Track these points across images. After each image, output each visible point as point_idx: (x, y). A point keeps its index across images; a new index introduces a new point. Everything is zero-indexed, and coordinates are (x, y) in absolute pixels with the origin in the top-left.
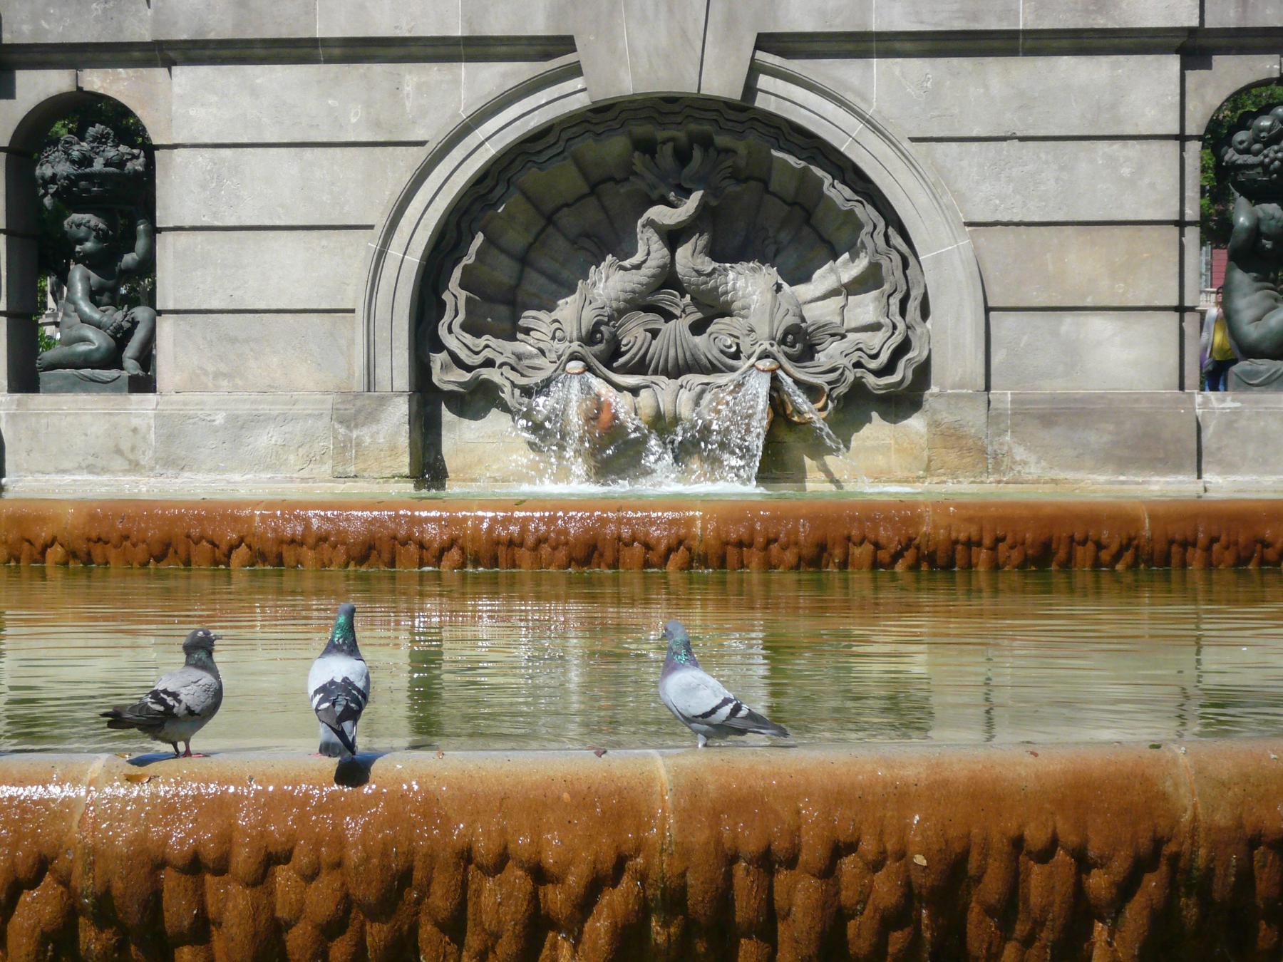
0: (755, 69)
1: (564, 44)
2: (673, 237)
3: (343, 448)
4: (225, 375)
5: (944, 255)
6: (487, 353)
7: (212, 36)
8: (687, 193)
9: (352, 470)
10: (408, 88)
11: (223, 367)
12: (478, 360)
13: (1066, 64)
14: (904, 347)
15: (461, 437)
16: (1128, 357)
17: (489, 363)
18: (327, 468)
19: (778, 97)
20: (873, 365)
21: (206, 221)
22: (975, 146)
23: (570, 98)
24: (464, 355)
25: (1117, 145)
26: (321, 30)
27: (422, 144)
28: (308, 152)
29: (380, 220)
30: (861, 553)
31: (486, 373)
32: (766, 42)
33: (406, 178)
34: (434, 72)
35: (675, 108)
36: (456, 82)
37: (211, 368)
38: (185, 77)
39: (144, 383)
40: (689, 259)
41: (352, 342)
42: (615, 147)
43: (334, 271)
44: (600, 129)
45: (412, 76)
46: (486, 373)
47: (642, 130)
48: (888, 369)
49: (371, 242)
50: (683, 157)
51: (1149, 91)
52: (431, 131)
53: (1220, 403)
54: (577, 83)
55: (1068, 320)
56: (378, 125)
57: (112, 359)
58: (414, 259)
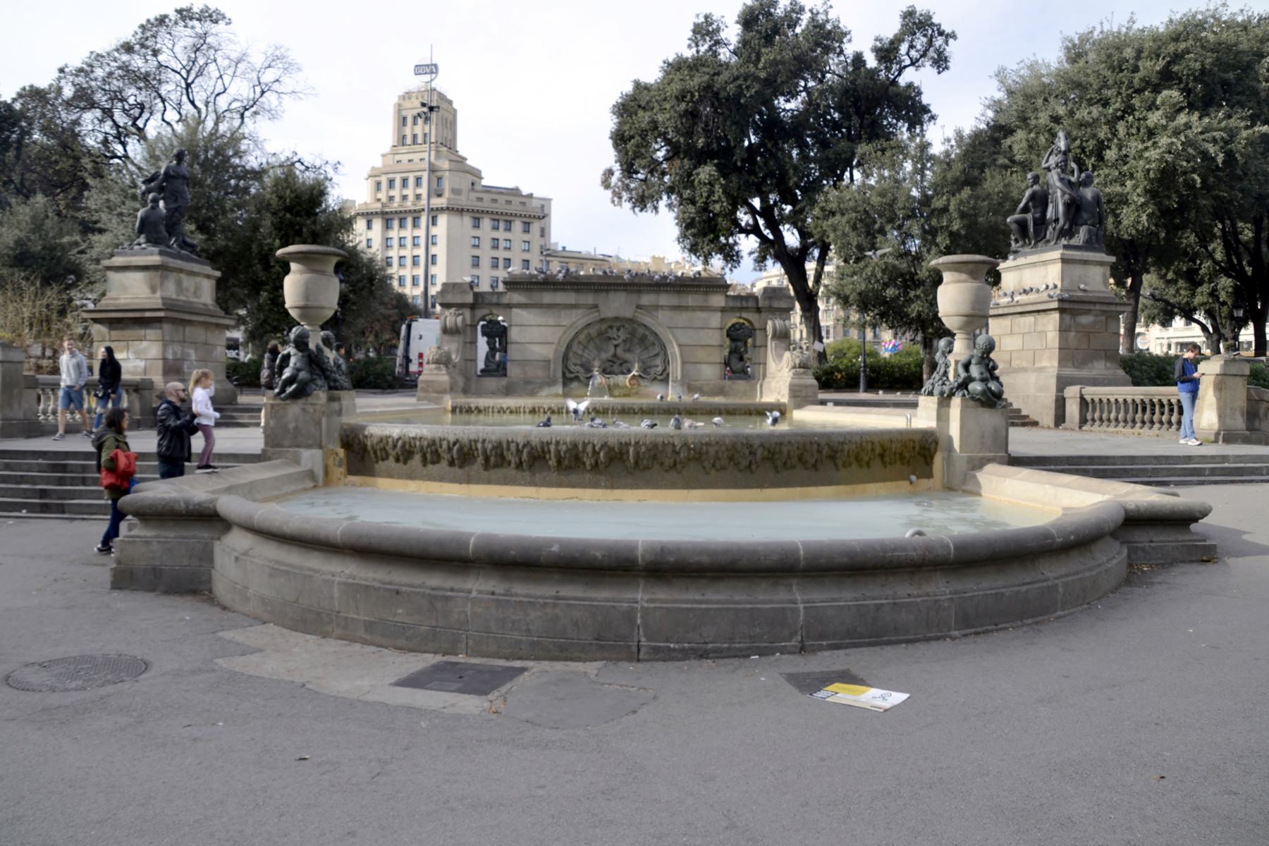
1: (596, 306)
2: (616, 346)
5: (674, 351)
16: (710, 372)
39: (505, 375)
42: (604, 326)
51: (715, 320)
53: (728, 383)
57: (497, 370)
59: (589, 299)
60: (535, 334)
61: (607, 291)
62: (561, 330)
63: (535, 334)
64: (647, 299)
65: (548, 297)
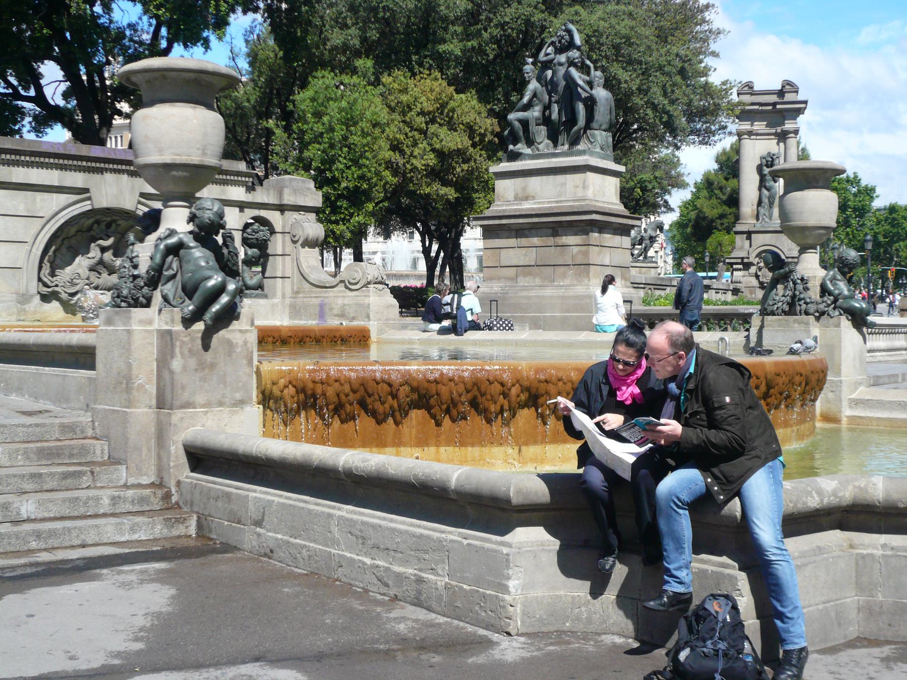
1: (87, 190)
3: (19, 313)
8: (109, 237)
9: (22, 318)
17: (57, 286)
18: (14, 317)
23: (86, 206)
24: (49, 283)
29: (29, 239)
30: (270, 339)
31: (56, 289)
33: (40, 228)
34: (46, 196)
40: (108, 256)
45: (39, 196)
46: (56, 289)
47: (98, 217)
49: (27, 247)
50: (109, 225)
52: (48, 215)
54: (89, 202)
56: (28, 210)
58: (39, 253)
59: (76, 179)
61: (101, 171)
62: (39, 223)
65: (19, 174)
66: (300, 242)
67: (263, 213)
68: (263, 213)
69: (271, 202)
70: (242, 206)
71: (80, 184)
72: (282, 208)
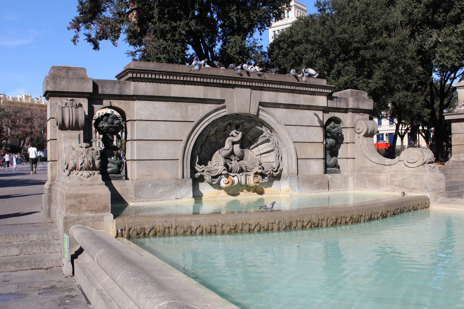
0: (259, 110)
1: (223, 101)
2: (234, 143)
4: (149, 175)
6: (203, 169)
7: (147, 95)
10: (189, 109)
11: (148, 173)
12: (201, 170)
13: (307, 111)
14: (278, 167)
15: (206, 189)
16: (317, 167)
19: (264, 116)
20: (275, 170)
21: (144, 138)
22: (293, 127)
23: (222, 113)
25: (314, 127)
26: (173, 95)
27: (193, 122)
28: (167, 123)
29: (185, 139)
31: (202, 174)
32: (261, 104)
33: (190, 129)
34: (195, 105)
35: (239, 116)
36: (200, 108)
37: (145, 174)
38: (137, 104)
41: (178, 167)
43: (176, 150)
44: (224, 120)
45: (191, 106)
48: (276, 171)
49: (183, 144)
53: (329, 176)
55: (308, 160)
59: (215, 93)
60: (162, 130)
61: (233, 86)
63: (162, 130)
64: (268, 96)
65: (176, 90)
66: (363, 133)
67: (337, 115)
68: (337, 115)
69: (342, 107)
70: (326, 110)
71: (218, 97)
72: (346, 111)
